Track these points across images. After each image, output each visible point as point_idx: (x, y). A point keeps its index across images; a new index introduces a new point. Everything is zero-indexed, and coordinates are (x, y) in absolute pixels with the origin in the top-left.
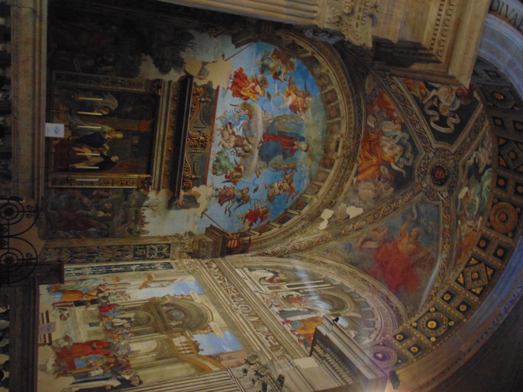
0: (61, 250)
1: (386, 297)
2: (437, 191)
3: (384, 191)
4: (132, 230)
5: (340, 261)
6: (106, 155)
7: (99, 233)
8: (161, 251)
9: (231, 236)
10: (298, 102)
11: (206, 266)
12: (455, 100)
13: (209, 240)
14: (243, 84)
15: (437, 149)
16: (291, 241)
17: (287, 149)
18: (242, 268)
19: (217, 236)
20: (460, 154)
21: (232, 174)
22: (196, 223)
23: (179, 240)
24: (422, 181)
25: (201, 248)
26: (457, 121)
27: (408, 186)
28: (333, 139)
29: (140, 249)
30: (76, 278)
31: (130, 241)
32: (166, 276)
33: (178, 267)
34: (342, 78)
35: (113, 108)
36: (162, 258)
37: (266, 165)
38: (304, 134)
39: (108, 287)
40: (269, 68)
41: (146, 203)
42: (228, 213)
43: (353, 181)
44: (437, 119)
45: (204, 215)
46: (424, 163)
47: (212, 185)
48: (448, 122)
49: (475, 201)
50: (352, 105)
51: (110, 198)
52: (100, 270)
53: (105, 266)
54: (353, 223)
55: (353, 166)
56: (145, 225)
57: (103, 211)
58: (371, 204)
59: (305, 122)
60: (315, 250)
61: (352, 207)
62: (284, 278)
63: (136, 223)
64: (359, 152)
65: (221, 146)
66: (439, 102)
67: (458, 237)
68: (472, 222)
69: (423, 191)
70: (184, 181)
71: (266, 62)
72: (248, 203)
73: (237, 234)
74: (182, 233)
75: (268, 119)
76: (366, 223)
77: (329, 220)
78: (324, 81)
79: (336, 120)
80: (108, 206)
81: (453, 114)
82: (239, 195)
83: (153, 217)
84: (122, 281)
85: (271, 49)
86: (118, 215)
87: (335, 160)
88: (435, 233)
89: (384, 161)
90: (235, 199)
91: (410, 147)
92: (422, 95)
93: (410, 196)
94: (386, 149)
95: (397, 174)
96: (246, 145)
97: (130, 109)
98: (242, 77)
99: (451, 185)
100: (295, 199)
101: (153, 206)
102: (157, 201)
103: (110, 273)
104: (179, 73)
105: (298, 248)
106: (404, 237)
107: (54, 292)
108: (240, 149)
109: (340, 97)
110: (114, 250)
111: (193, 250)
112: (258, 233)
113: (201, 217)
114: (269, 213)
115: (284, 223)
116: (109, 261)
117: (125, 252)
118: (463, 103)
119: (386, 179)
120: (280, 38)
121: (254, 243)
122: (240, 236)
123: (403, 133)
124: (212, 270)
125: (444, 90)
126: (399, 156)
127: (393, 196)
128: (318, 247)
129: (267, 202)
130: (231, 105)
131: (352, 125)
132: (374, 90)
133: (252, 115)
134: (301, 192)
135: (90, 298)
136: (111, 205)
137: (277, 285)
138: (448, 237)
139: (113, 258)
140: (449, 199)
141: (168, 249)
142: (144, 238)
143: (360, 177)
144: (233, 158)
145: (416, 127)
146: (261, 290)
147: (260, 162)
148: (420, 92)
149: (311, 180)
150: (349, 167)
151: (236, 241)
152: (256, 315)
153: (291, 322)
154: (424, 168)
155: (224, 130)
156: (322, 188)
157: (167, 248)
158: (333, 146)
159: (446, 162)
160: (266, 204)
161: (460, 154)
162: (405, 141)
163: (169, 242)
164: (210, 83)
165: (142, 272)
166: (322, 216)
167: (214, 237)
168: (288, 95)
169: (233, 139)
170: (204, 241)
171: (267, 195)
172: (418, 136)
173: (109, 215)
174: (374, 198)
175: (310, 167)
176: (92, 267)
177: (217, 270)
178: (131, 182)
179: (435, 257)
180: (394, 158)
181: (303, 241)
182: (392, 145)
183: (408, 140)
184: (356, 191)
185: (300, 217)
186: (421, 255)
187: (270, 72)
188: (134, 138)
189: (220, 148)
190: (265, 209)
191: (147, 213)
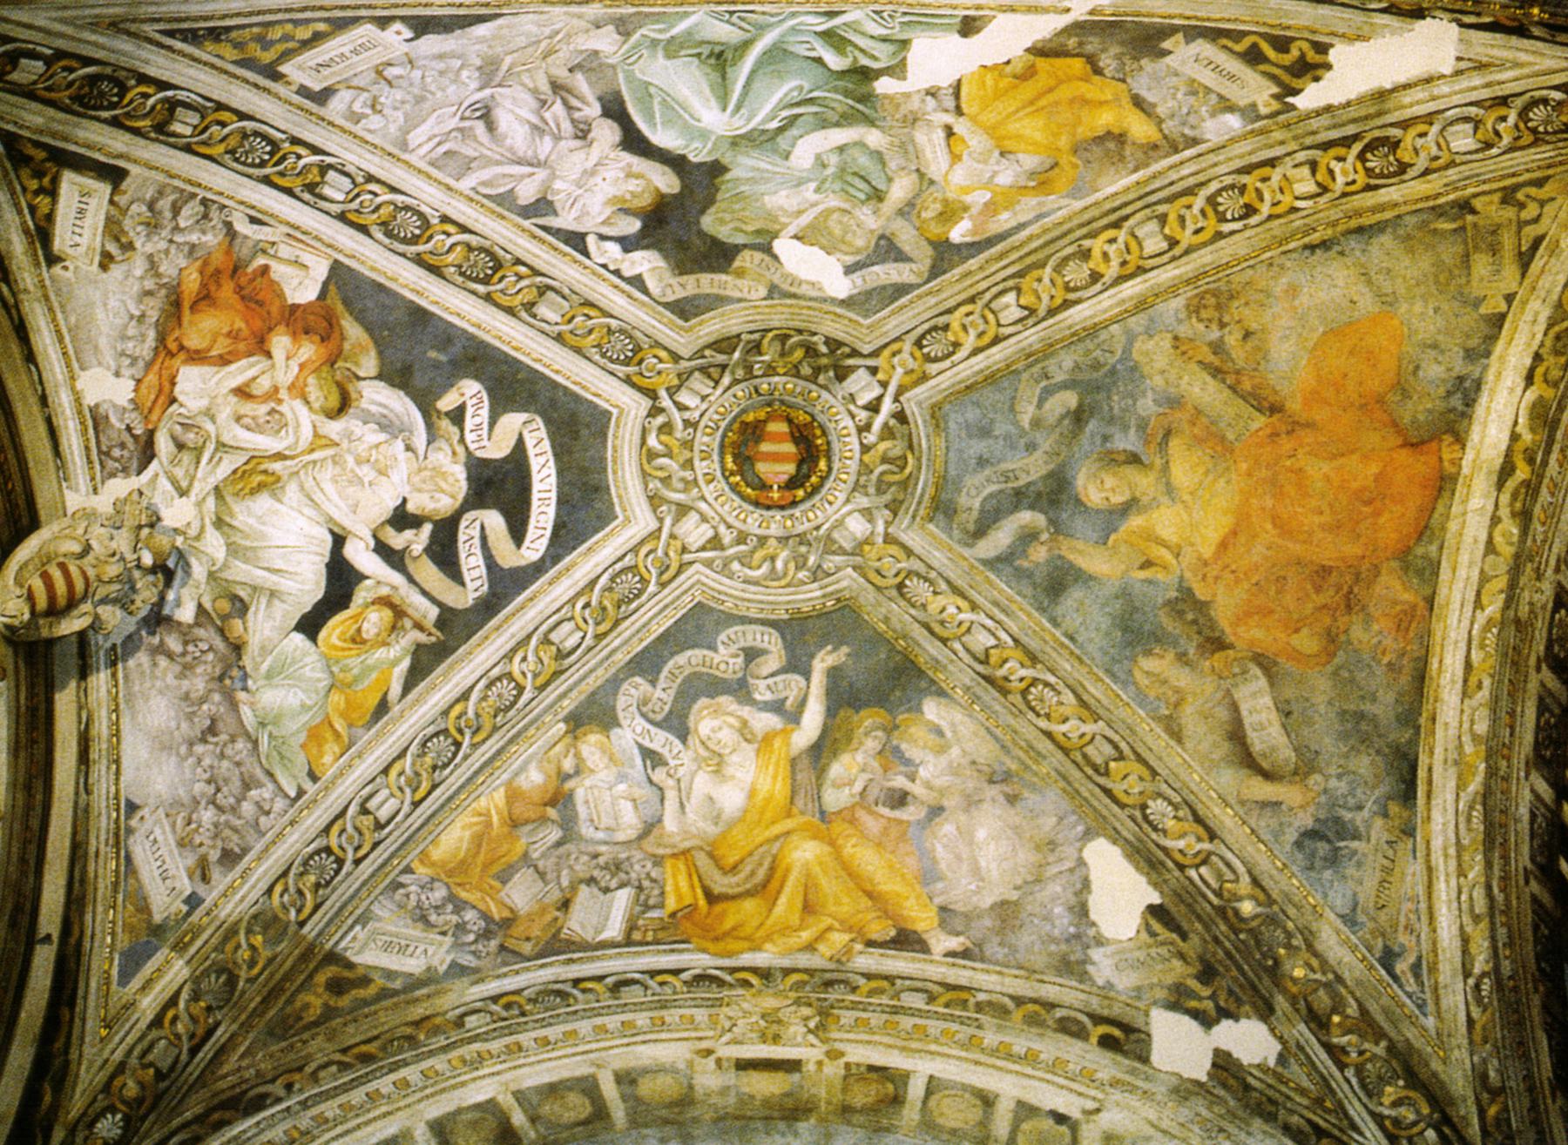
1: (1500, 485)
2: (866, 449)
3: (955, 752)
12: (367, 418)
15: (654, 501)
20: (637, 349)
26: (470, 391)
27: (886, 620)
43: (948, 954)
44: (494, 520)
46: (744, 560)
48: (497, 449)
49: (821, 163)
54: (1181, 867)
55: (869, 976)
58: (1047, 808)
60: (1411, 1034)
66: (402, 519)
67: (1028, 207)
68: (920, 136)
69: (888, 524)
76: (1160, 795)
77: (1206, 1021)
81: (445, 424)
87: (848, 1066)
88: (1068, 363)
91: (681, 659)
93: (935, 593)
94: (731, 799)
105: (1431, 1134)
118: (369, 364)
119: (891, 756)
123: (621, 715)
125: (328, 487)
126: (746, 711)
127: (967, 689)
128: (1380, 1019)
138: (1058, 269)
140: (875, 354)
143: (923, 919)
145: (570, 643)
150: (885, 1000)
154: (773, 559)
156: (1032, 1098)
159: (701, 440)
161: (635, 356)
162: (663, 694)
172: (617, 623)
174: (1012, 799)
179: (1177, 303)
180: (768, 739)
181: (1378, 1119)
183: (653, 683)
184: (1007, 913)
186: (1203, 390)
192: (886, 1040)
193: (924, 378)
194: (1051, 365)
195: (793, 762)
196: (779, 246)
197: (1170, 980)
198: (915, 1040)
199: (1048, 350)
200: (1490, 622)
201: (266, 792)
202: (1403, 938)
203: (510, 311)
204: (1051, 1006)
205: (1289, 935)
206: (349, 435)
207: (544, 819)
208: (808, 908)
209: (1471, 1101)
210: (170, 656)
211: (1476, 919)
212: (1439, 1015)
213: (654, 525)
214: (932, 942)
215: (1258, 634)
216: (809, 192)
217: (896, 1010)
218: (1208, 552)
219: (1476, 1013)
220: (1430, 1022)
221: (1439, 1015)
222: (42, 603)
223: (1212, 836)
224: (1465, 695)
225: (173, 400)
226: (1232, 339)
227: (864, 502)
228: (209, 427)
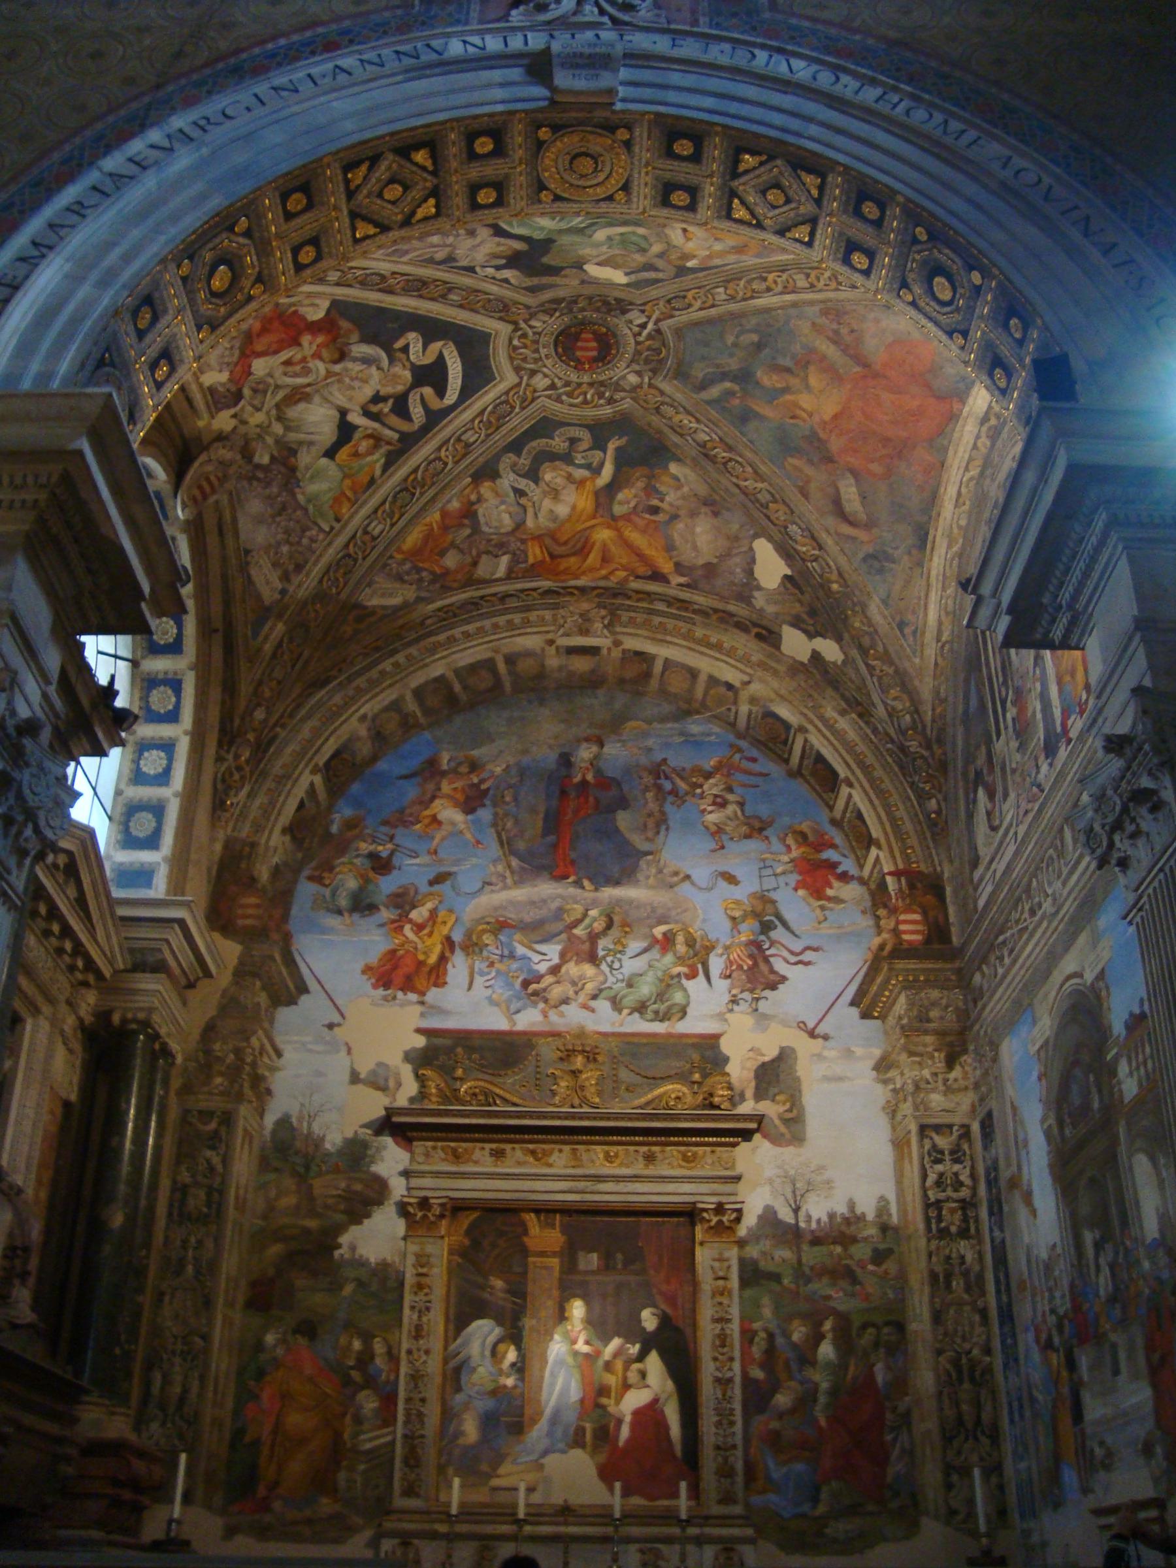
2: (638, 343)
3: (686, 489)
4: (876, 1251)
5: (924, 583)
6: (638, 1346)
9: (885, 935)
10: (455, 789)
11: (980, 1004)
12: (355, 360)
14: (408, 960)
15: (517, 370)
16: (892, 741)
17: (597, 800)
18: (976, 889)
19: (887, 981)
21: (681, 960)
22: (848, 1053)
23: (905, 1100)
24: (624, 390)
25: (932, 1025)
26: (413, 339)
27: (649, 424)
28: (560, 669)
29: (939, 1219)
31: (914, 1255)
34: (383, 673)
35: (498, 1331)
36: (970, 1148)
37: (650, 857)
38: (547, 756)
40: (361, 889)
41: (786, 1215)
42: (808, 956)
44: (428, 391)
45: (817, 1031)
46: (570, 395)
47: (721, 1017)
48: (429, 359)
50: (457, 632)
51: (772, 1326)
54: (804, 560)
55: (637, 592)
56: (858, 1211)
57: (817, 1345)
58: (734, 522)
59: (512, 760)
60: (907, 664)
61: (758, 572)
62: (983, 749)
63: (854, 1240)
64: (593, 584)
65: (593, 1004)
66: (377, 398)
70: (713, 1106)
71: (343, 902)
72: (773, 895)
73: (878, 918)
74: (881, 1094)
75: (508, 874)
77: (811, 636)
78: (392, 725)
79: (502, 667)
80: (798, 1332)
82: (748, 930)
83: (831, 1188)
85: (306, 890)
86: (829, 1297)
87: (624, 651)
88: (754, 321)
89: (598, 505)
90: (762, 937)
91: (534, 444)
92: (376, 447)
94: (562, 510)
95: (623, 461)
96: (590, 925)
97: (499, 1284)
98: (388, 967)
99: (604, 309)
100: (754, 753)
101: (794, 1192)
102: (778, 1180)
104: (385, 1148)
105: (908, 717)
106: (797, 405)
108: (603, 944)
109: (437, 670)
112: (874, 852)
113: (826, 1038)
114: (805, 827)
115: (835, 774)
116: (984, 1313)
118: (355, 337)
119: (650, 490)
120: (276, 872)
121: (906, 858)
122: (885, 906)
123: (502, 472)
124: (985, 986)
125: (337, 394)
126: (570, 469)
127: (694, 459)
128: (893, 655)
129: (767, 838)
130: (469, 988)
131: (517, 618)
132: (400, 578)
133: (498, 921)
134: (731, 737)
135: (1065, 1374)
136: (796, 1323)
137: (997, 770)
139: (973, 1303)
142: (903, 1211)
143: (667, 567)
144: (630, 966)
146: (1011, 825)
147: (640, 876)
148: (370, 452)
149: (689, 713)
150: (645, 605)
151: (902, 917)
152: (1061, 830)
153: (1066, 714)
154: (585, 394)
155: (546, 1001)
156: (716, 674)
157: (934, 1135)
158: (581, 665)
159: (543, 340)
160: (774, 840)
162: (524, 461)
163: (914, 1128)
164: (408, 1057)
165: (1006, 1209)
166: (805, 657)
168: (435, 820)
169: (572, 969)
171: (745, 841)
173: (828, 1325)
174: (716, 514)
175: (649, 723)
178: (717, 1264)
180: (581, 483)
182: (545, 494)
183: (519, 455)
184: (710, 570)
185: (810, 727)
187: (371, 887)
188: (582, 1266)
189: (603, 1005)
190: (790, 841)
191: (818, 1209)
192: (645, 633)
193: (672, 316)
194: (744, 321)
195: (597, 494)
196: (586, 267)
197: (794, 612)
198: (660, 634)
199: (742, 315)
200: (971, 479)
201: (314, 532)
202: (910, 617)
203: (433, 299)
204: (731, 615)
205: (854, 605)
206: (346, 370)
207: (462, 525)
208: (605, 559)
209: (929, 707)
210: (258, 480)
211: (947, 613)
212: (922, 657)
213: (517, 380)
214: (671, 578)
215: (852, 460)
216: (604, 249)
217: (652, 612)
218: (827, 417)
219: (940, 660)
220: (917, 661)
221: (922, 657)
222: (199, 498)
223: (821, 548)
224: (957, 505)
225: (250, 374)
226: (844, 331)
227: (637, 368)
228: (271, 381)
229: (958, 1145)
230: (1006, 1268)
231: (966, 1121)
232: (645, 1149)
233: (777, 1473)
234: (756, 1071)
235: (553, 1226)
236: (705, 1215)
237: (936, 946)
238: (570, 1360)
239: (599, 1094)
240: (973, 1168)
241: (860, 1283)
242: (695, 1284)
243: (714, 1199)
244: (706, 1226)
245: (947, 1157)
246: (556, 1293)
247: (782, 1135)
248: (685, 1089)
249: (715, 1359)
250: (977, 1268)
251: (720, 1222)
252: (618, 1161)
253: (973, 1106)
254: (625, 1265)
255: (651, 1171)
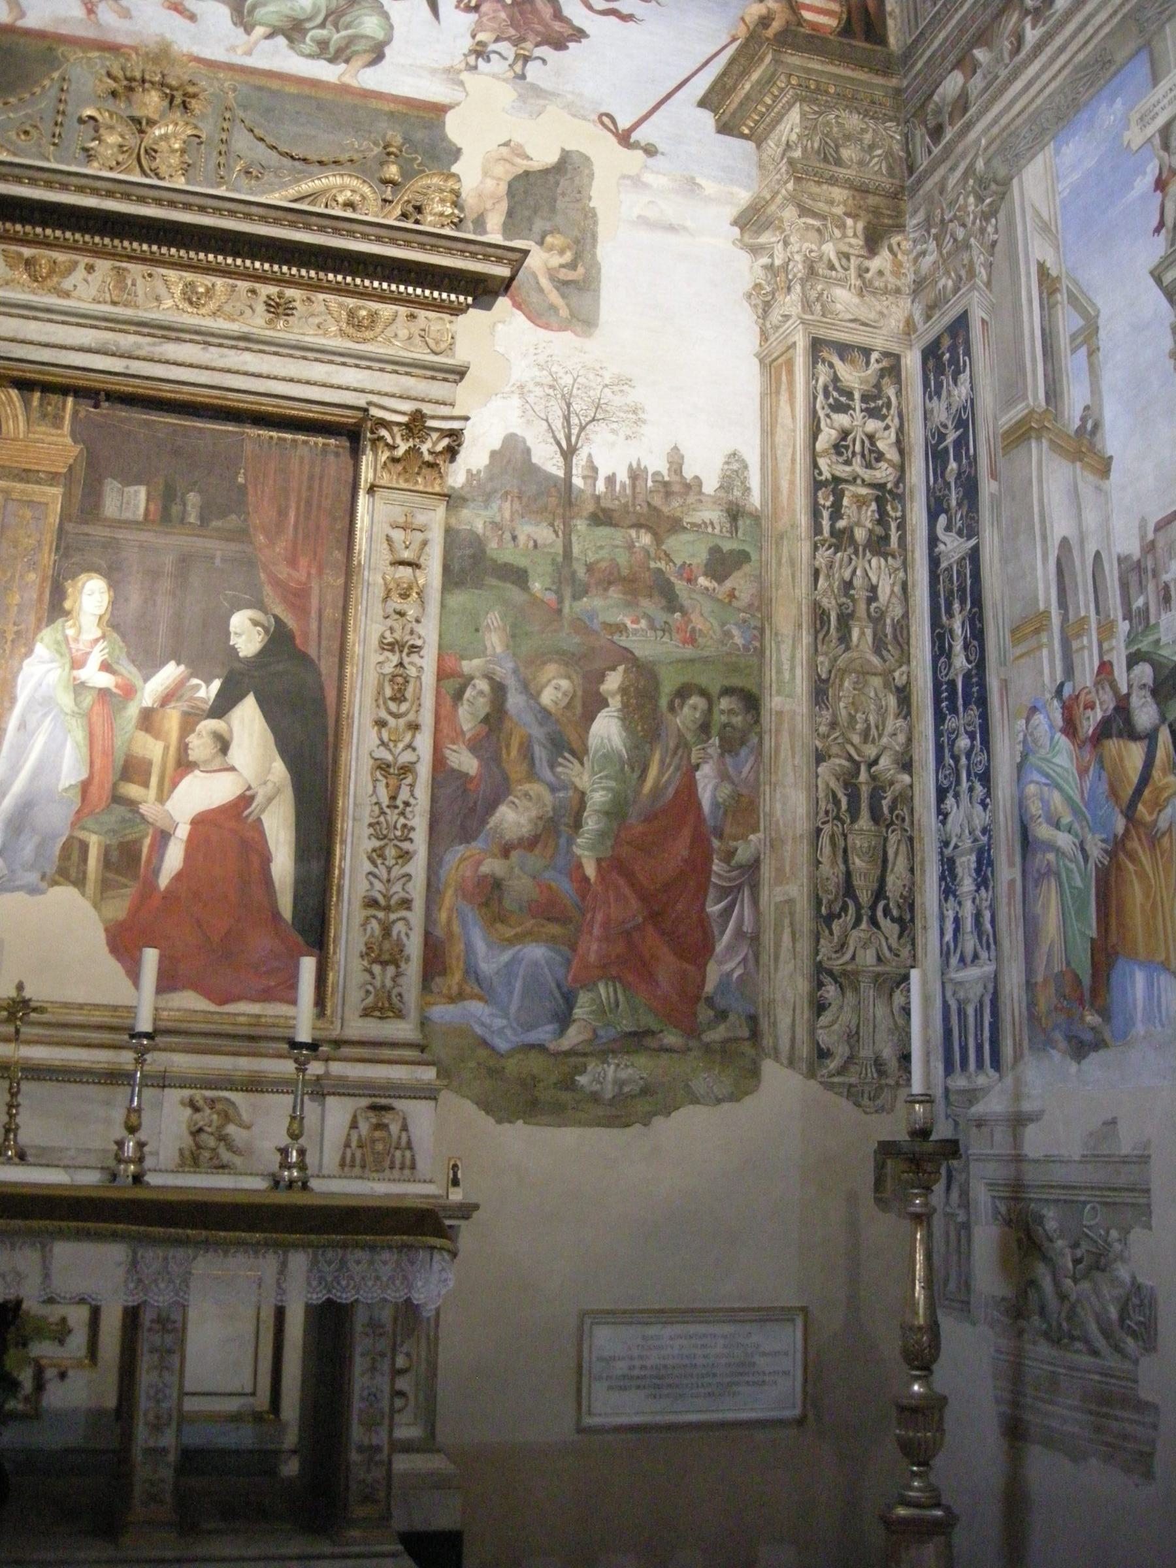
0: (830, 973)
4: (715, 551)
6: (216, 684)
7: (732, 744)
8: (857, 396)
11: (949, 134)
13: (792, 123)
19: (770, 80)
22: (691, 186)
23: (789, 288)
25: (842, 172)
29: (836, 513)
30: (1012, 882)
31: (786, 571)
32: (1018, 339)
33: (956, 289)
36: (899, 393)
39: (1086, 675)
41: (547, 459)
45: (634, 137)
47: (451, 75)
51: (504, 671)
52: (963, 742)
53: (939, 717)
56: (688, 473)
57: (589, 717)
63: (676, 526)
83: (640, 422)
84: (1046, 594)
86: (621, 629)
101: (567, 419)
103: (982, 685)
107: (1105, 1013)
110: (841, 663)
111: (855, 217)
113: (650, 151)
116: (904, 696)
117: (853, 600)
136: (551, 669)
139: (887, 675)
141: (842, 359)
157: (836, 360)
163: (801, 341)
165: (987, 488)
167: (775, 98)
170: (797, 154)
173: (613, 682)
176: (941, 794)
177: (980, 54)
178: (398, 535)
188: (111, 506)
229: (878, 386)
230: (978, 602)
231: (895, 348)
232: (273, 290)
233: (489, 961)
234: (510, 185)
235: (57, 421)
236: (383, 432)
237: (861, 44)
238: (66, 700)
239: (186, 169)
240: (900, 430)
241: (682, 609)
242: (349, 570)
243: (408, 407)
244: (384, 456)
245: (857, 404)
246: (47, 558)
247: (553, 308)
248: (366, 190)
249: (381, 724)
250: (897, 611)
251: (414, 451)
252: (213, 305)
253: (910, 324)
254: (204, 520)
255: (281, 331)
